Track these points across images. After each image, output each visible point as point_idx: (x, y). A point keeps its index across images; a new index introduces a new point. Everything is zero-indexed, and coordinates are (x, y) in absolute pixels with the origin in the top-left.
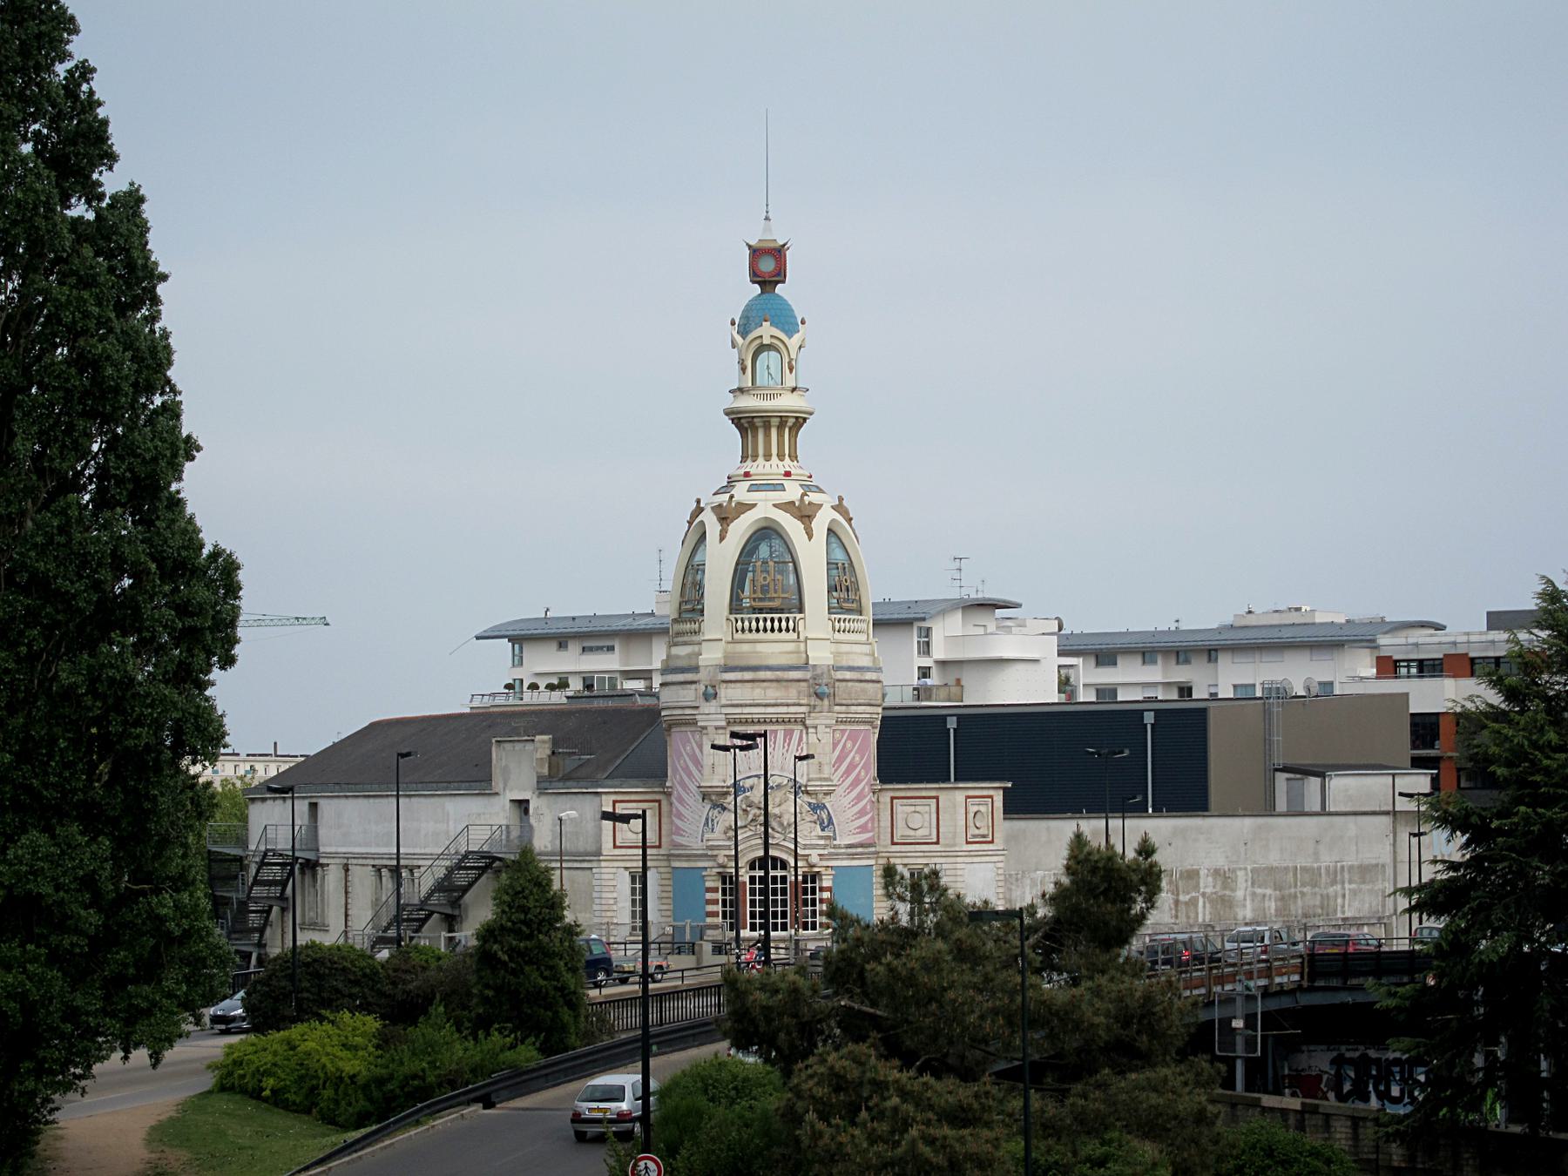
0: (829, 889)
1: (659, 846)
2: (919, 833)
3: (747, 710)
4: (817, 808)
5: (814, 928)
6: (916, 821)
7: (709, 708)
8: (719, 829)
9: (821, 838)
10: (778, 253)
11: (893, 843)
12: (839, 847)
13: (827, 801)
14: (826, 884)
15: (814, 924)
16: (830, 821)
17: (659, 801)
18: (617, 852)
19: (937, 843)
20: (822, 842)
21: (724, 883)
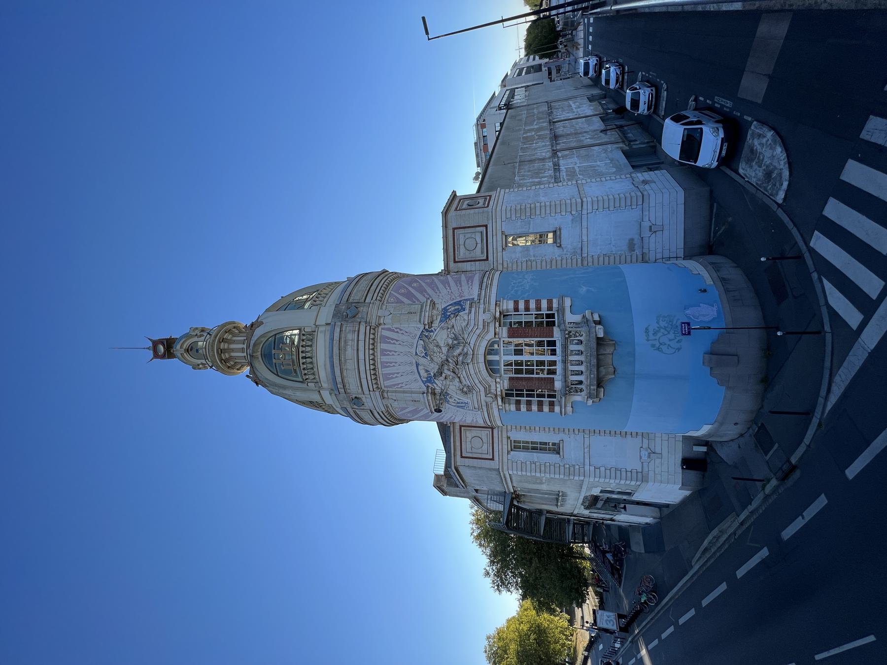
0: (516, 303)
1: (492, 428)
2: (479, 241)
3: (363, 375)
4: (446, 316)
5: (553, 316)
6: (470, 244)
7: (368, 404)
8: (464, 399)
9: (470, 312)
10: (155, 344)
11: (487, 259)
12: (479, 295)
13: (441, 306)
14: (511, 305)
15: (548, 316)
16: (456, 304)
17: (461, 427)
18: (496, 458)
19: (486, 226)
20: (473, 310)
21: (512, 395)
